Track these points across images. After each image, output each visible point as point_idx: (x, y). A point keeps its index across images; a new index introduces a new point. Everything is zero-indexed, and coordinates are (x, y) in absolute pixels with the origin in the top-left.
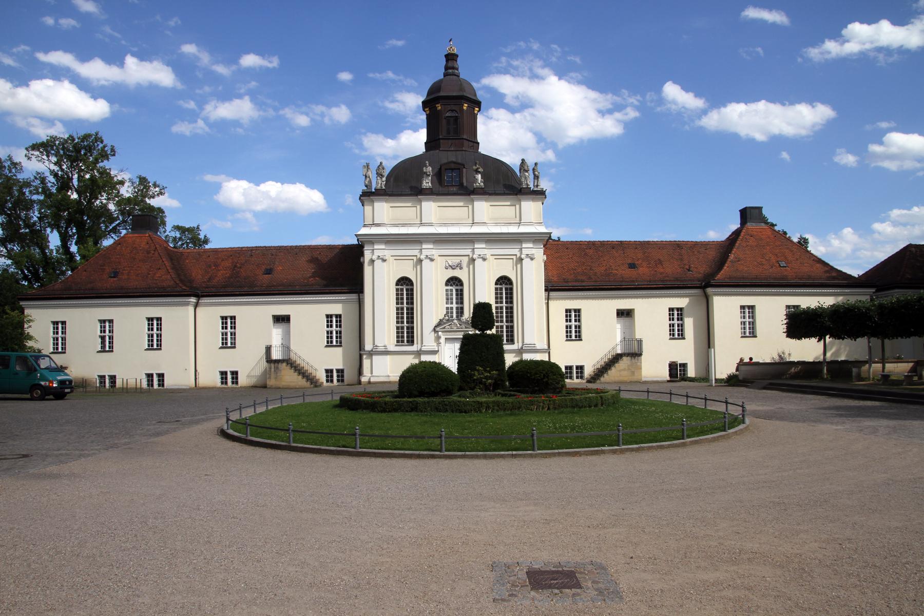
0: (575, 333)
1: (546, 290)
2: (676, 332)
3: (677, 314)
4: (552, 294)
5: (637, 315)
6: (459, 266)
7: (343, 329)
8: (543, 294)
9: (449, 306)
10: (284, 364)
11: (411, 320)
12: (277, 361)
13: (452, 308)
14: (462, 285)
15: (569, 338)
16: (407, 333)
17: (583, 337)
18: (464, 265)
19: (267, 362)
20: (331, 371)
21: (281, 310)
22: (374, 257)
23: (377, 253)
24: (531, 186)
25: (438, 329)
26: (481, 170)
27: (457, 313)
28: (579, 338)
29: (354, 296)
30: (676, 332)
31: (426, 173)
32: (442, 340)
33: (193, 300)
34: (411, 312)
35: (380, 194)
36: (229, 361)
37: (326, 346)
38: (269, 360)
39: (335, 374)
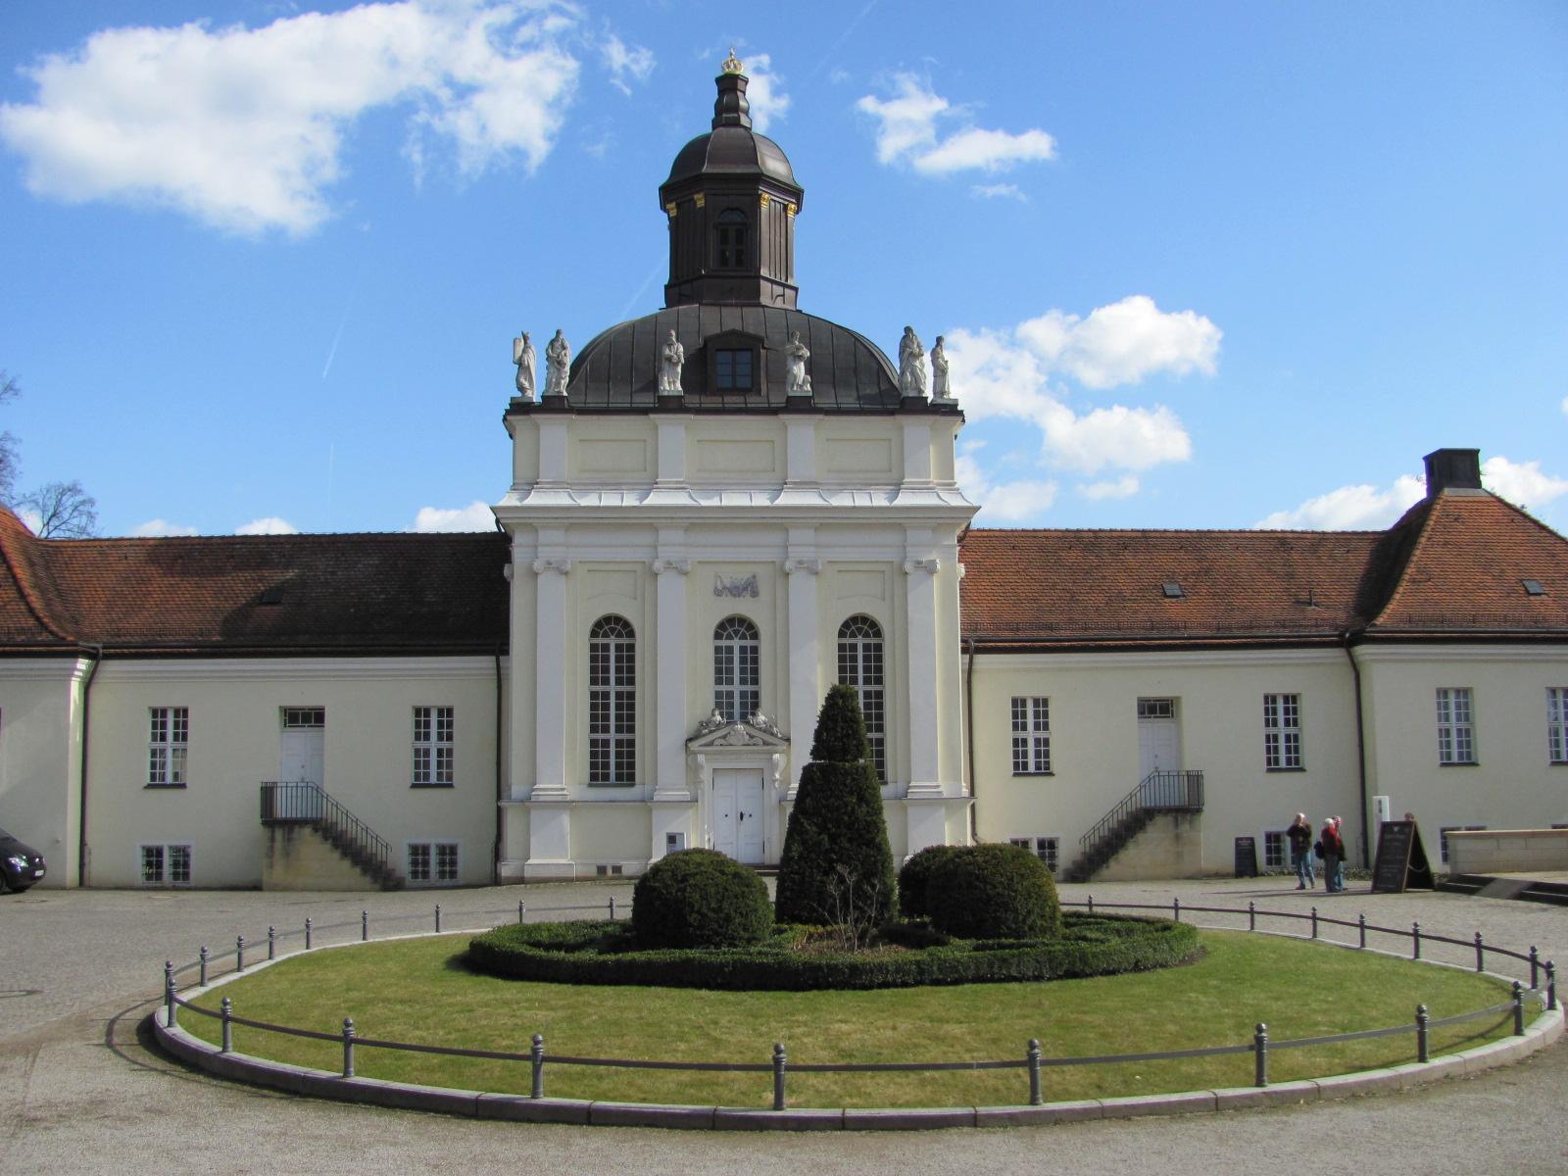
0: (1032, 761)
1: (965, 651)
2: (1283, 756)
3: (1283, 709)
4: (981, 660)
5: (1186, 711)
6: (749, 588)
7: (457, 744)
8: (961, 660)
9: (724, 688)
10: (307, 831)
11: (627, 722)
12: (290, 824)
13: (730, 694)
14: (755, 636)
15: (1020, 769)
16: (614, 761)
17: (1054, 768)
18: (764, 588)
19: (265, 823)
20: (426, 850)
21: (303, 698)
22: (537, 565)
23: (544, 553)
24: (929, 394)
25: (694, 746)
26: (807, 353)
27: (743, 705)
28: (1044, 770)
29: (485, 663)
30: (1283, 756)
31: (669, 359)
32: (706, 775)
33: (83, 664)
34: (627, 702)
35: (552, 405)
36: (169, 822)
37: (414, 786)
38: (269, 820)
39: (434, 858)
